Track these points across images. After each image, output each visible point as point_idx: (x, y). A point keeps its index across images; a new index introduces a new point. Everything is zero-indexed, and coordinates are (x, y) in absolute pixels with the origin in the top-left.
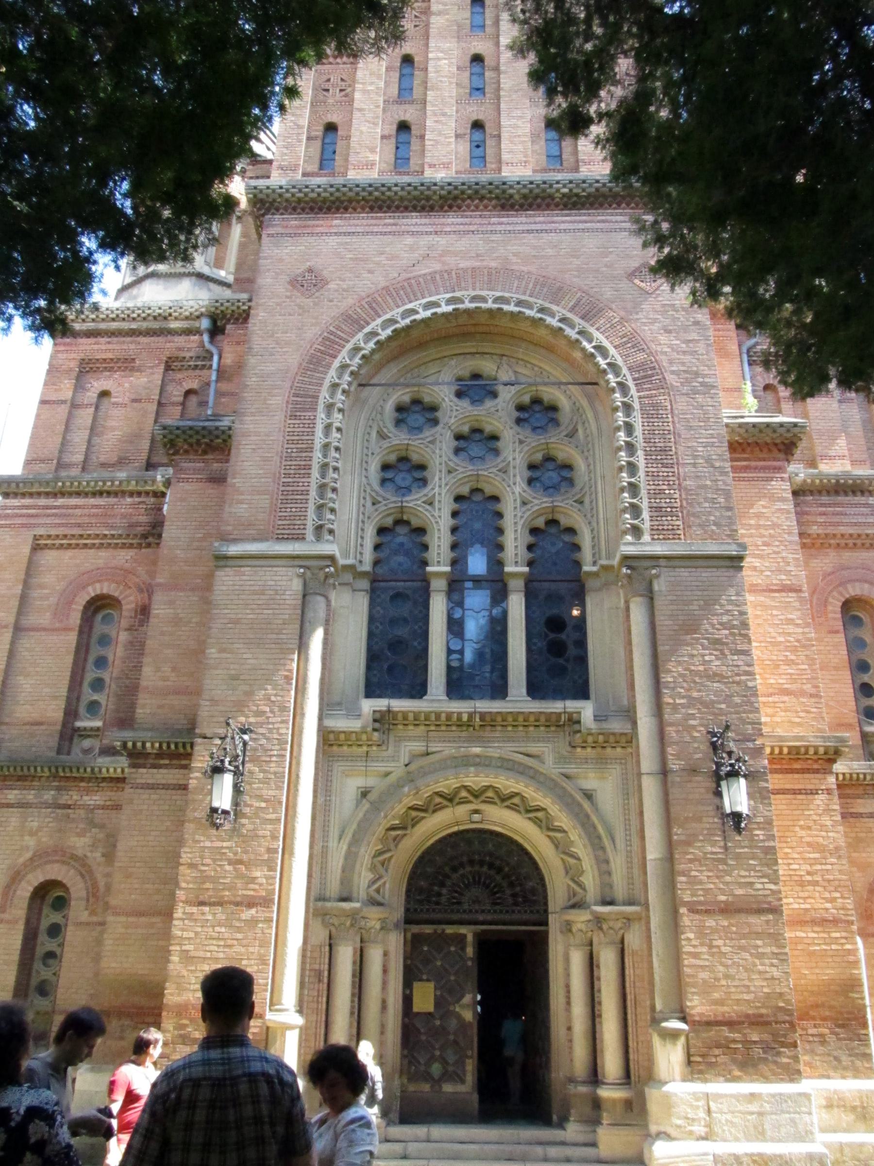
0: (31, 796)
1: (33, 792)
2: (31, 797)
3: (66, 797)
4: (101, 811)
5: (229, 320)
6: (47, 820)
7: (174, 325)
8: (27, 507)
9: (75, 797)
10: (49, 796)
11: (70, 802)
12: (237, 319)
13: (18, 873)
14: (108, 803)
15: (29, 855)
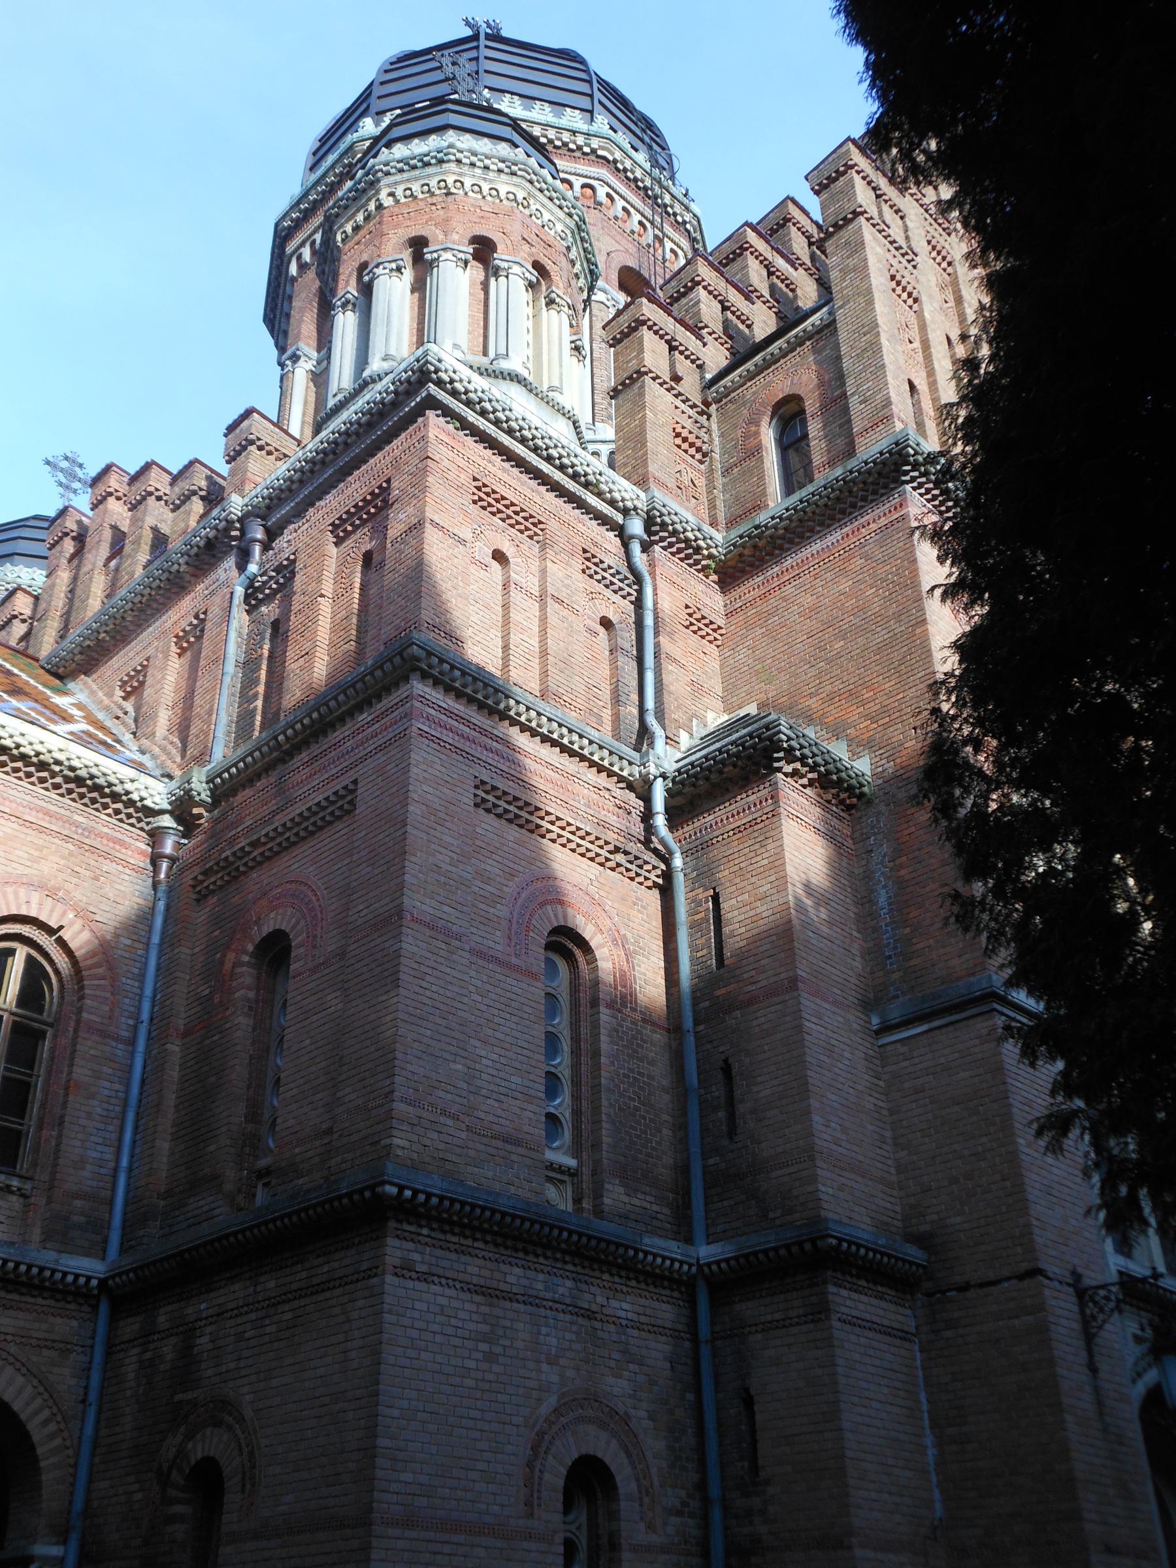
0: (539, 1281)
1: (541, 1277)
2: (540, 1286)
3: (587, 1297)
4: (636, 1333)
5: (662, 539)
6: (568, 1336)
7: (592, 500)
8: (459, 718)
9: (599, 1299)
10: (564, 1288)
11: (594, 1307)
12: (671, 545)
13: (541, 1434)
14: (643, 1319)
15: (552, 1400)
